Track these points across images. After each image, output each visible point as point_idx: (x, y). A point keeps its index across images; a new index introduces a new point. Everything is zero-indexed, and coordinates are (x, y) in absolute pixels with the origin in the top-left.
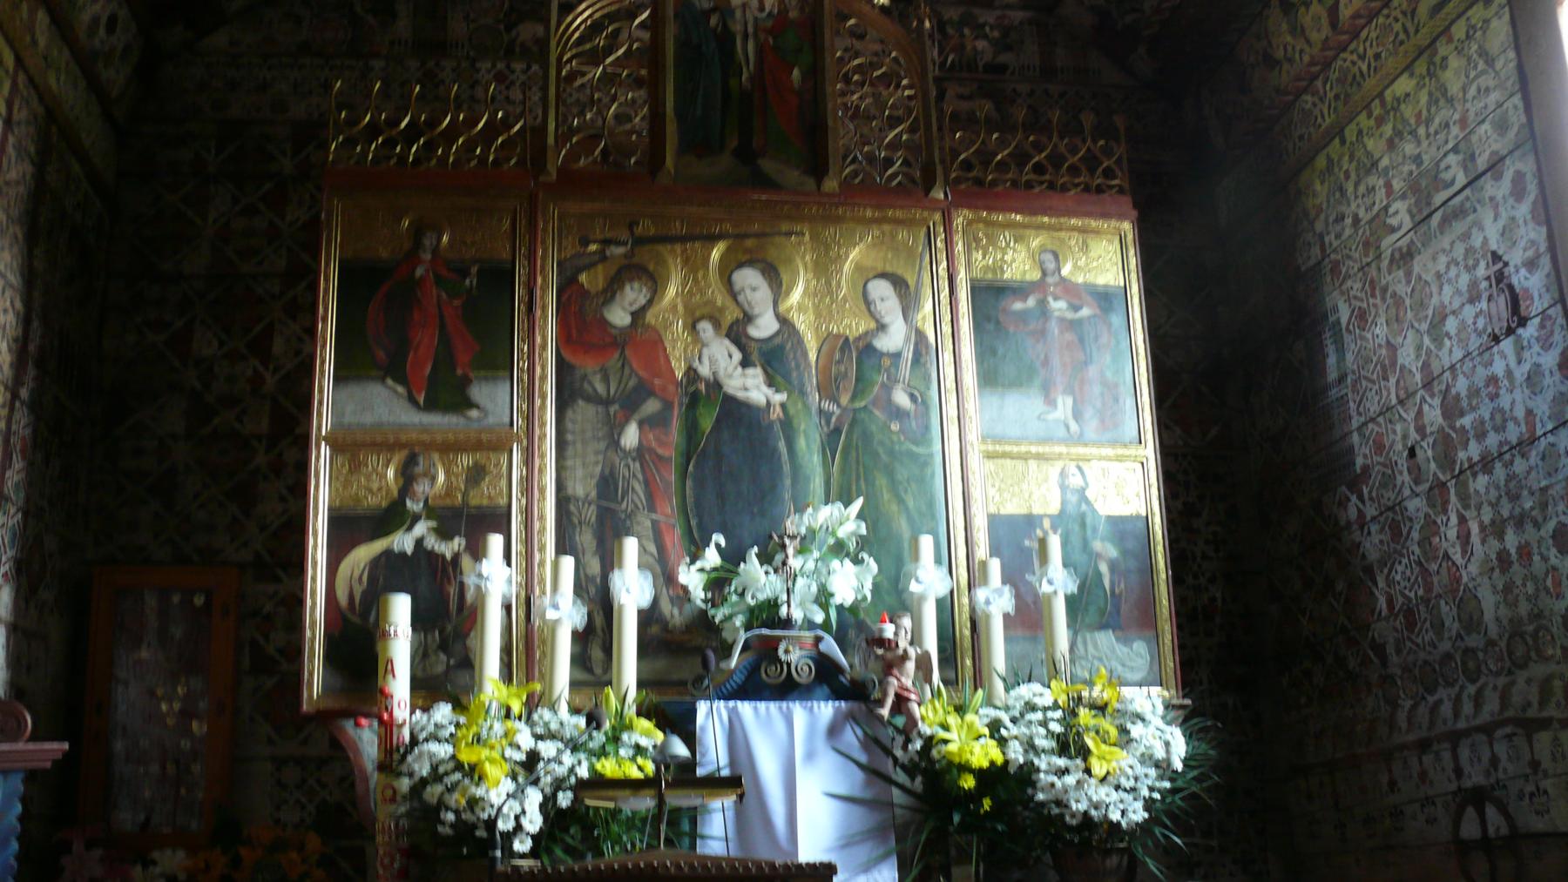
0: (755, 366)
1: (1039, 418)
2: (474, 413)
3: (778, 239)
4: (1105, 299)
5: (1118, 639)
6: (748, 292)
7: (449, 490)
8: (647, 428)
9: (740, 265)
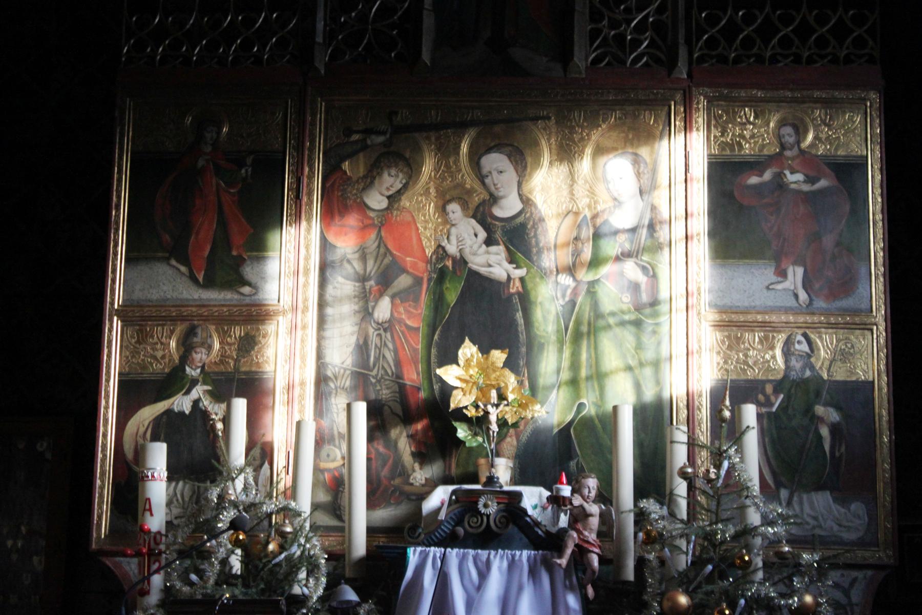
0: (498, 244)
1: (768, 288)
2: (246, 290)
3: (530, 123)
4: (848, 171)
5: (835, 500)
6: (495, 174)
7: (223, 356)
8: (398, 301)
9: (489, 150)
